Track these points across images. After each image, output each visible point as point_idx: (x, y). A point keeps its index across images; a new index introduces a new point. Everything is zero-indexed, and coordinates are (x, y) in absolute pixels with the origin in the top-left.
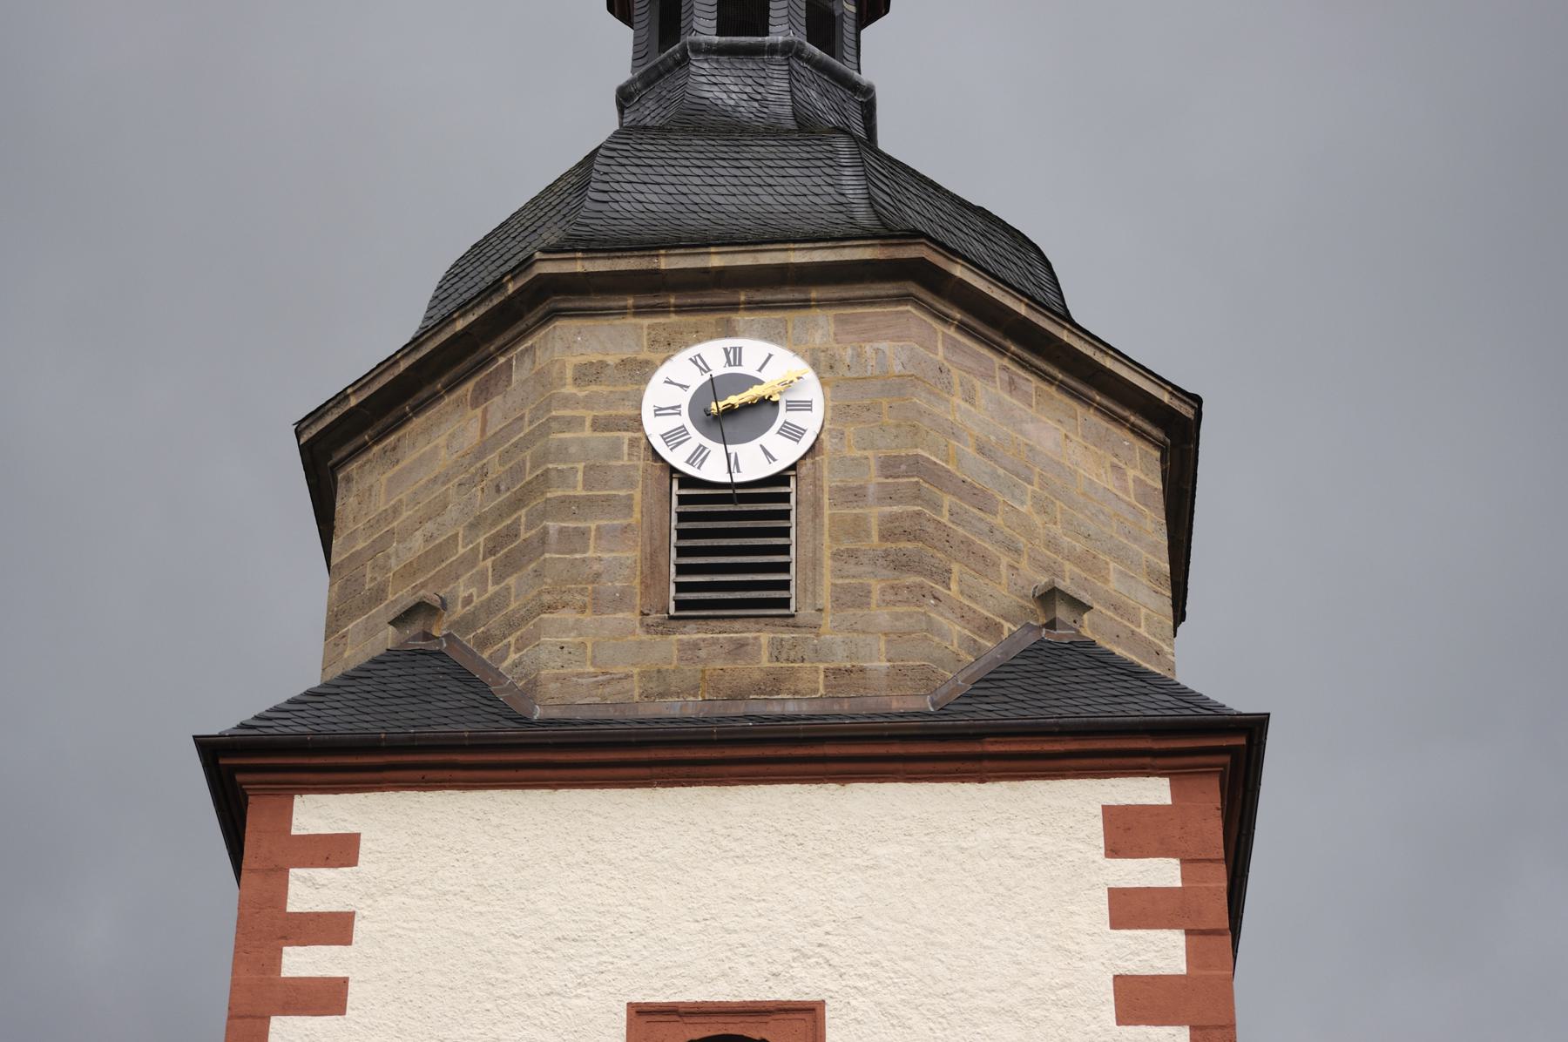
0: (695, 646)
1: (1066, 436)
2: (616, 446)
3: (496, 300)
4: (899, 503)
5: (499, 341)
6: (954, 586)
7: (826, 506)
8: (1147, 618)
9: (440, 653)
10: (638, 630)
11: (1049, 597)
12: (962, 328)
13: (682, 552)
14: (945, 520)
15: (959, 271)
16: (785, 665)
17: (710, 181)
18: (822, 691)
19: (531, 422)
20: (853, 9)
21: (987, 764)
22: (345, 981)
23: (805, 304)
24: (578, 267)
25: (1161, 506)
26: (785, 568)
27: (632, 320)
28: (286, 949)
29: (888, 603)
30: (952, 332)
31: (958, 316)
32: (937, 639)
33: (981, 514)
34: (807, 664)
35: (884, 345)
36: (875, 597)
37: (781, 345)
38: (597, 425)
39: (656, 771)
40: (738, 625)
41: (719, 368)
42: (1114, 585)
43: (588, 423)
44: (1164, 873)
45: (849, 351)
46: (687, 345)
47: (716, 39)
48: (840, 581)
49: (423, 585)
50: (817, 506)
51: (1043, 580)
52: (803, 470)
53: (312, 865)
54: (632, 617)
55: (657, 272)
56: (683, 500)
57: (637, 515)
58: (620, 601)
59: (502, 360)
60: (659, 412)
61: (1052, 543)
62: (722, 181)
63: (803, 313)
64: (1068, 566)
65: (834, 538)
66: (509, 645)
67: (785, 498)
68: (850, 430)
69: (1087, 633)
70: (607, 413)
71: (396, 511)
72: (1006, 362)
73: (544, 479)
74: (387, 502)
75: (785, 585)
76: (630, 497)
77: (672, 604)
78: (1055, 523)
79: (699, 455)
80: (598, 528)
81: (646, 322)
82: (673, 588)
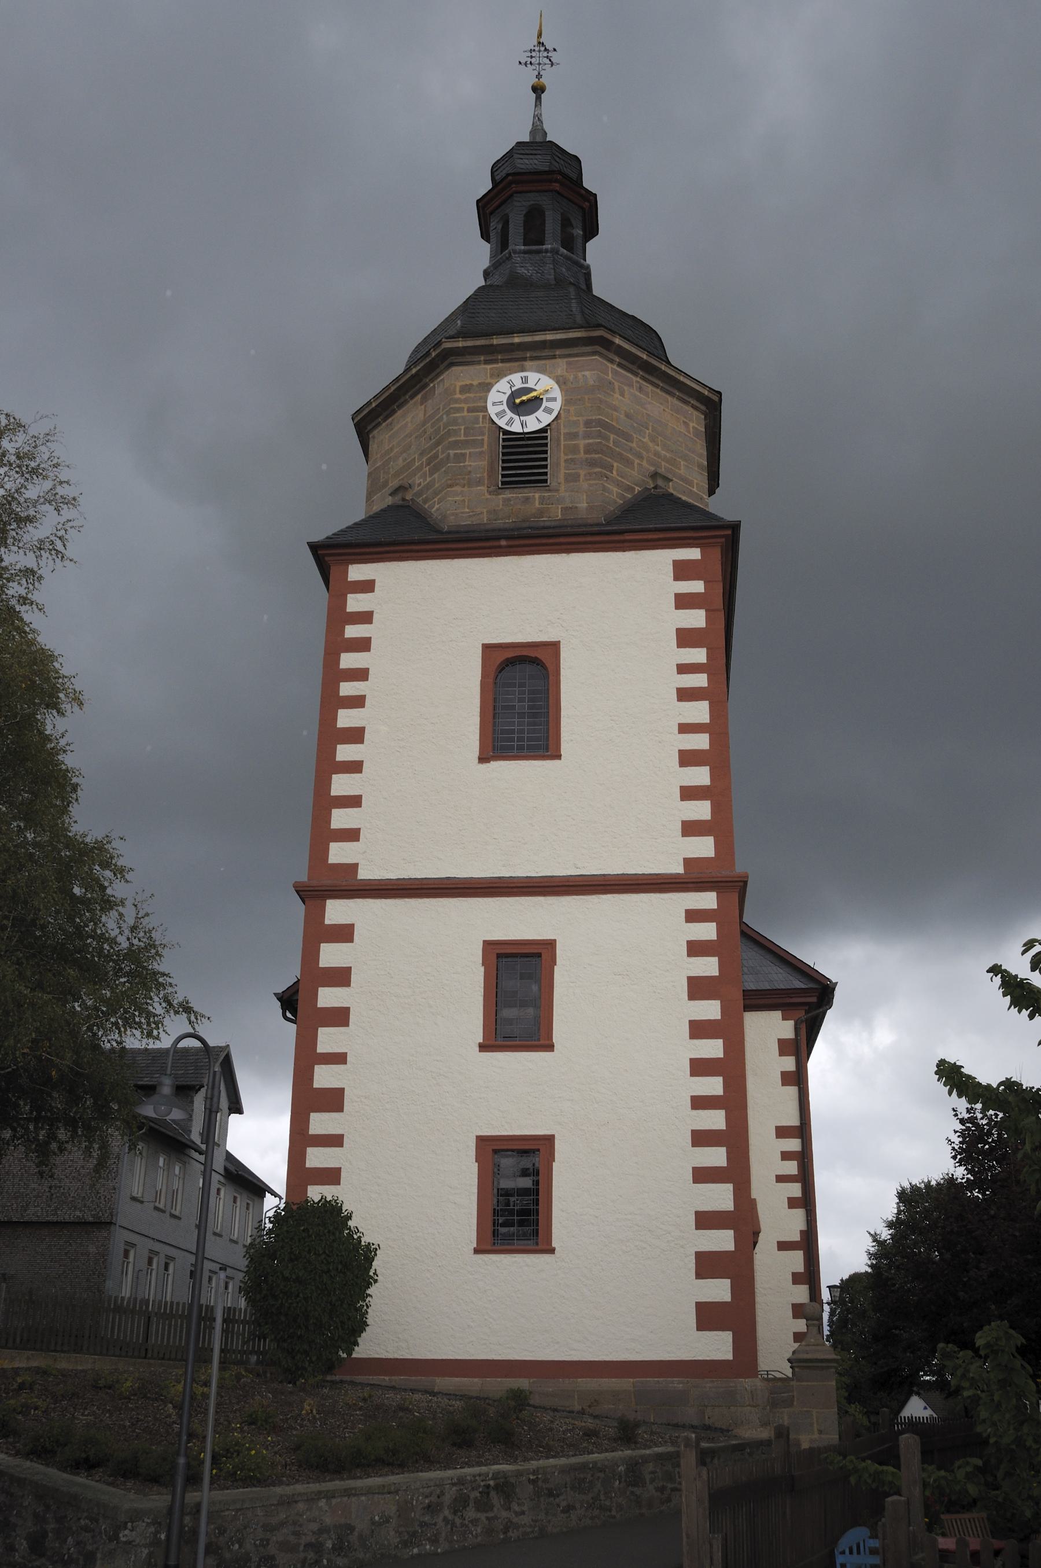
0: (509, 500)
1: (664, 410)
2: (477, 418)
3: (428, 360)
4: (593, 438)
6: (614, 472)
7: (562, 441)
8: (697, 484)
9: (409, 506)
10: (486, 494)
11: (654, 475)
12: (620, 365)
13: (504, 461)
14: (611, 445)
15: (617, 341)
16: (545, 506)
17: (516, 307)
18: (560, 516)
19: (443, 410)
20: (581, 233)
21: (626, 544)
22: (370, 638)
23: (554, 357)
24: (460, 344)
25: (704, 438)
26: (546, 467)
28: (346, 626)
29: (587, 480)
30: (615, 367)
31: (618, 360)
32: (607, 494)
33: (627, 443)
34: (554, 506)
35: (587, 373)
36: (582, 477)
37: (545, 374)
38: (469, 410)
39: (493, 550)
40: (526, 490)
41: (518, 385)
42: (682, 471)
43: (465, 409)
44: (697, 586)
45: (572, 376)
46: (506, 376)
47: (523, 247)
48: (567, 471)
49: (402, 479)
50: (558, 440)
51: (652, 469)
52: (553, 426)
54: (484, 488)
55: (492, 345)
56: (504, 440)
57: (486, 447)
58: (479, 482)
59: (432, 385)
60: (494, 404)
61: (656, 454)
62: (521, 307)
63: (553, 361)
64: (663, 463)
65: (566, 454)
66: (435, 502)
67: (546, 438)
68: (572, 409)
69: (671, 491)
70: (473, 405)
71: (392, 449)
72: (638, 379)
73: (449, 433)
74: (389, 445)
75: (546, 474)
76: (483, 440)
77: (500, 483)
78: (658, 446)
79: (510, 422)
80: (470, 453)
81: (489, 367)
82: (500, 476)
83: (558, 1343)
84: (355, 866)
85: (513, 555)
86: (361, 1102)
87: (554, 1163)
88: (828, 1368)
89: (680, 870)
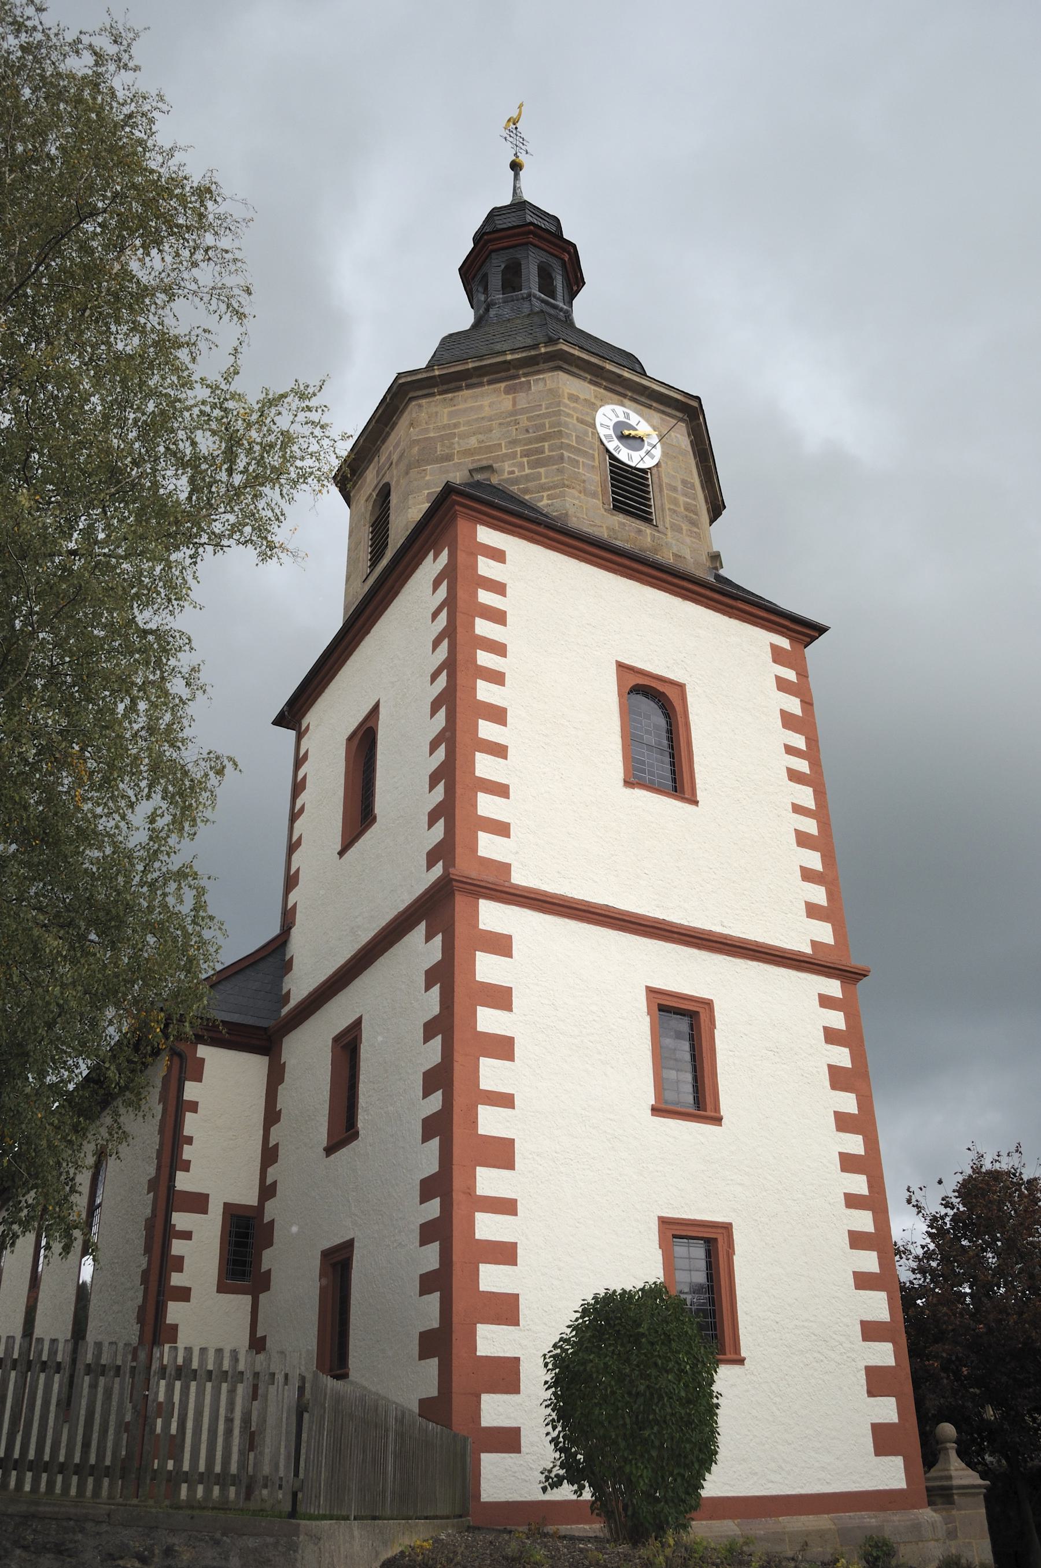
3: (533, 353)
5: (525, 370)
23: (650, 407)
27: (586, 384)
39: (621, 568)
46: (612, 404)
53: (487, 557)
79: (617, 448)
81: (593, 387)
83: (756, 1474)
84: (506, 868)
85: (636, 581)
86: (534, 1159)
87: (734, 1257)
88: (979, 1494)
89: (808, 950)
